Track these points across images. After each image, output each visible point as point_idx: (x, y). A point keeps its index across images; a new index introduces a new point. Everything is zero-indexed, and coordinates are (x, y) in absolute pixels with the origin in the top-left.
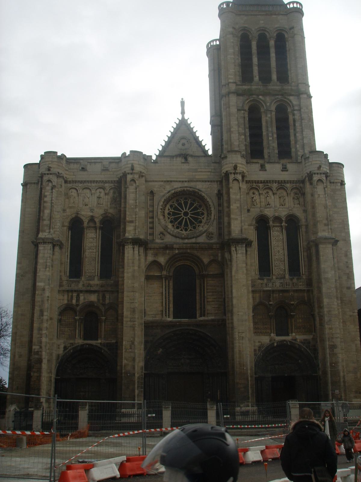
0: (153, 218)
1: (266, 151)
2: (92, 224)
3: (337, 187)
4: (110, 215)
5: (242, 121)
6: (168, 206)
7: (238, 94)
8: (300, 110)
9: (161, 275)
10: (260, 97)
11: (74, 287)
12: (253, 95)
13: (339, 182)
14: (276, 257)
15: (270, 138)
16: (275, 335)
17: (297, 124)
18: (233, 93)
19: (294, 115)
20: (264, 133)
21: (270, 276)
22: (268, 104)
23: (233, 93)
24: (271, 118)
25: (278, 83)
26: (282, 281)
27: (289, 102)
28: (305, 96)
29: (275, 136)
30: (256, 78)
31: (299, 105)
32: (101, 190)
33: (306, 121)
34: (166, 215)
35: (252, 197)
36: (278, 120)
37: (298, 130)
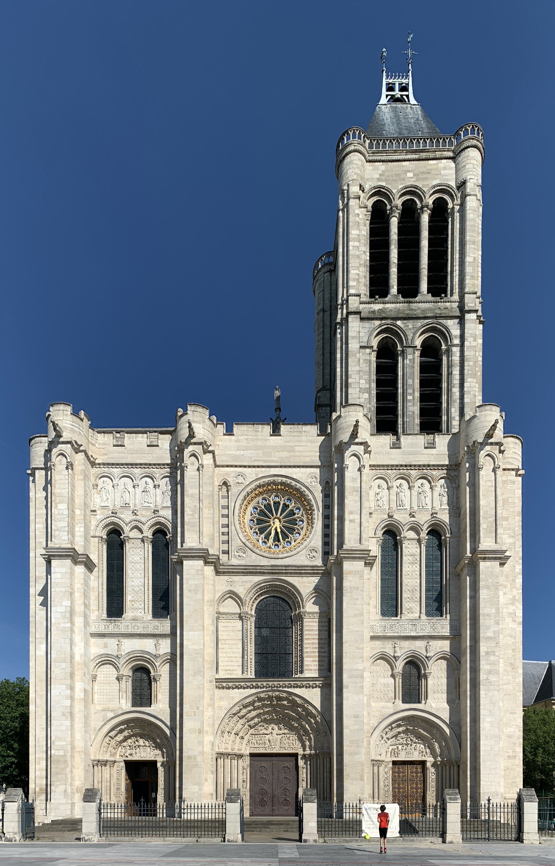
0: (228, 526)
2: (135, 534)
3: (509, 478)
4: (163, 520)
8: (462, 345)
9: (240, 614)
10: (399, 323)
11: (111, 628)
12: (385, 318)
13: (513, 470)
14: (408, 588)
17: (456, 371)
21: (397, 616)
25: (429, 297)
31: (462, 337)
35: (377, 492)
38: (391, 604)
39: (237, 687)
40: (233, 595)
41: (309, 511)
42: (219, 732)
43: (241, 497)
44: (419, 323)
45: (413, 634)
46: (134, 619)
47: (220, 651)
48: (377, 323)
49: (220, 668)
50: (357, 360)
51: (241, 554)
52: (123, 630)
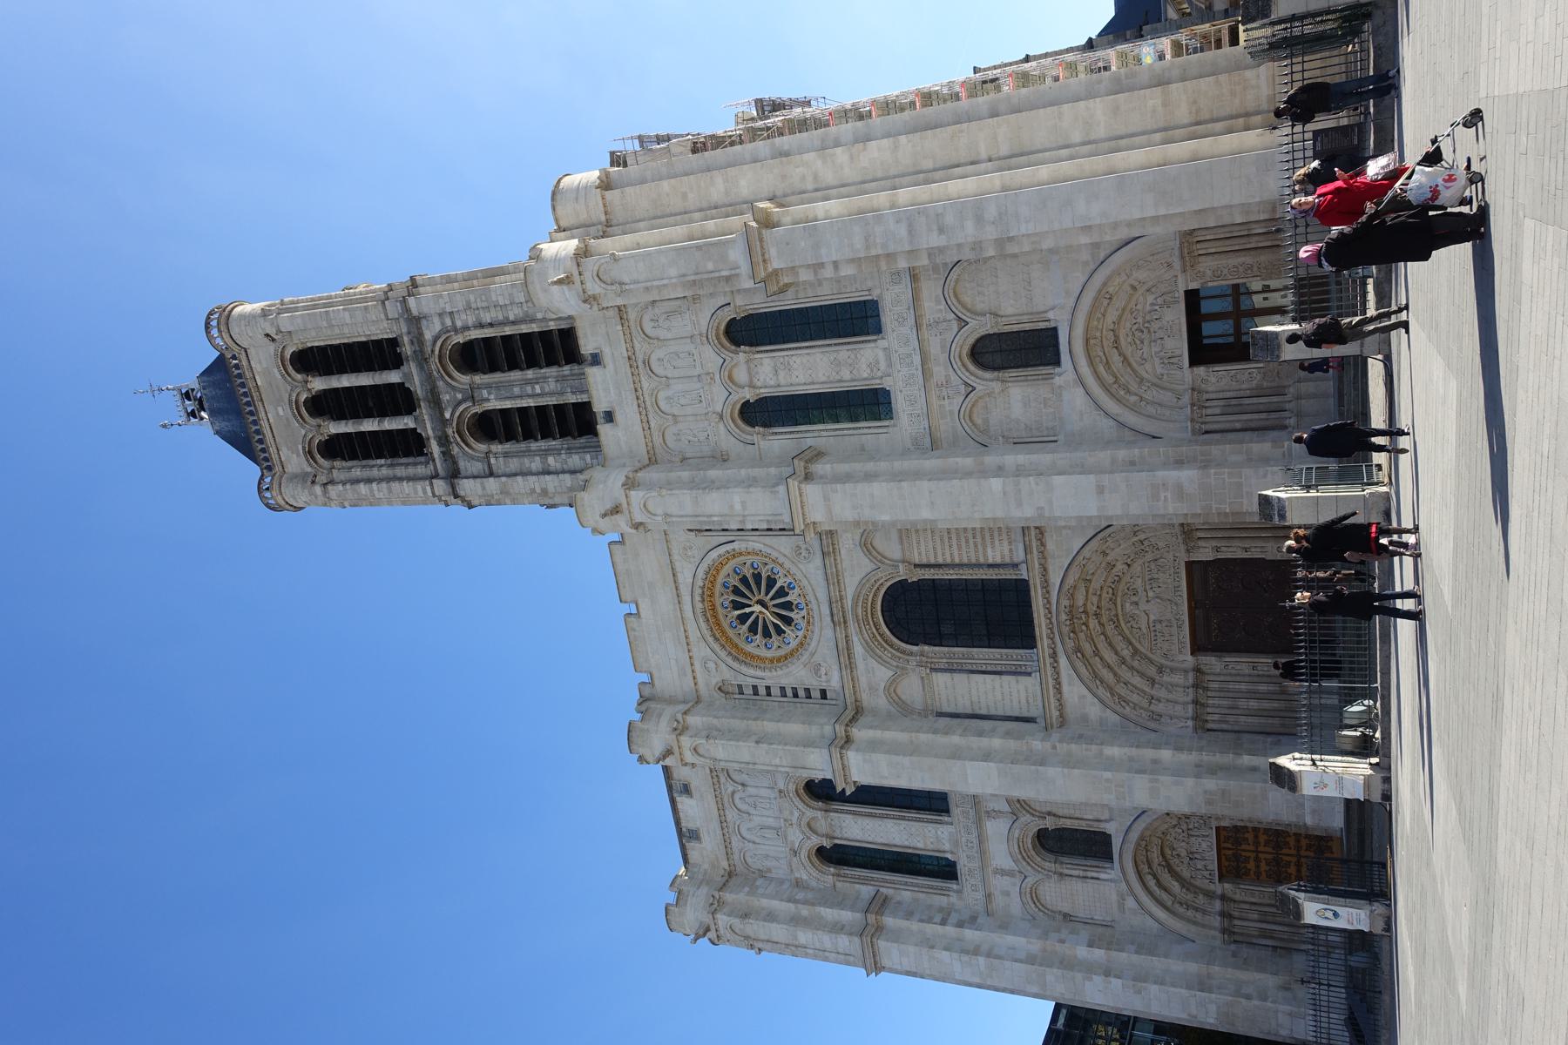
1: (572, 399)
4: (792, 787)
5: (514, 464)
6: (750, 648)
7: (454, 474)
8: (451, 313)
10: (447, 415)
12: (447, 437)
15: (538, 389)
16: (1057, 370)
18: (453, 487)
19: (466, 328)
20: (531, 403)
22: (459, 396)
23: (453, 487)
24: (489, 386)
25: (404, 368)
26: (895, 357)
27: (439, 343)
28: (411, 301)
29: (530, 374)
30: (405, 422)
32: (737, 796)
33: (472, 298)
34: (769, 654)
36: (493, 368)
37: (501, 317)
38: (869, 404)
39: (1059, 690)
40: (891, 688)
41: (735, 555)
42: (1152, 725)
43: (735, 665)
44: (440, 384)
45: (917, 359)
46: (956, 843)
47: (993, 712)
48: (455, 450)
49: (1025, 714)
50: (510, 480)
51: (823, 671)
52: (976, 864)
